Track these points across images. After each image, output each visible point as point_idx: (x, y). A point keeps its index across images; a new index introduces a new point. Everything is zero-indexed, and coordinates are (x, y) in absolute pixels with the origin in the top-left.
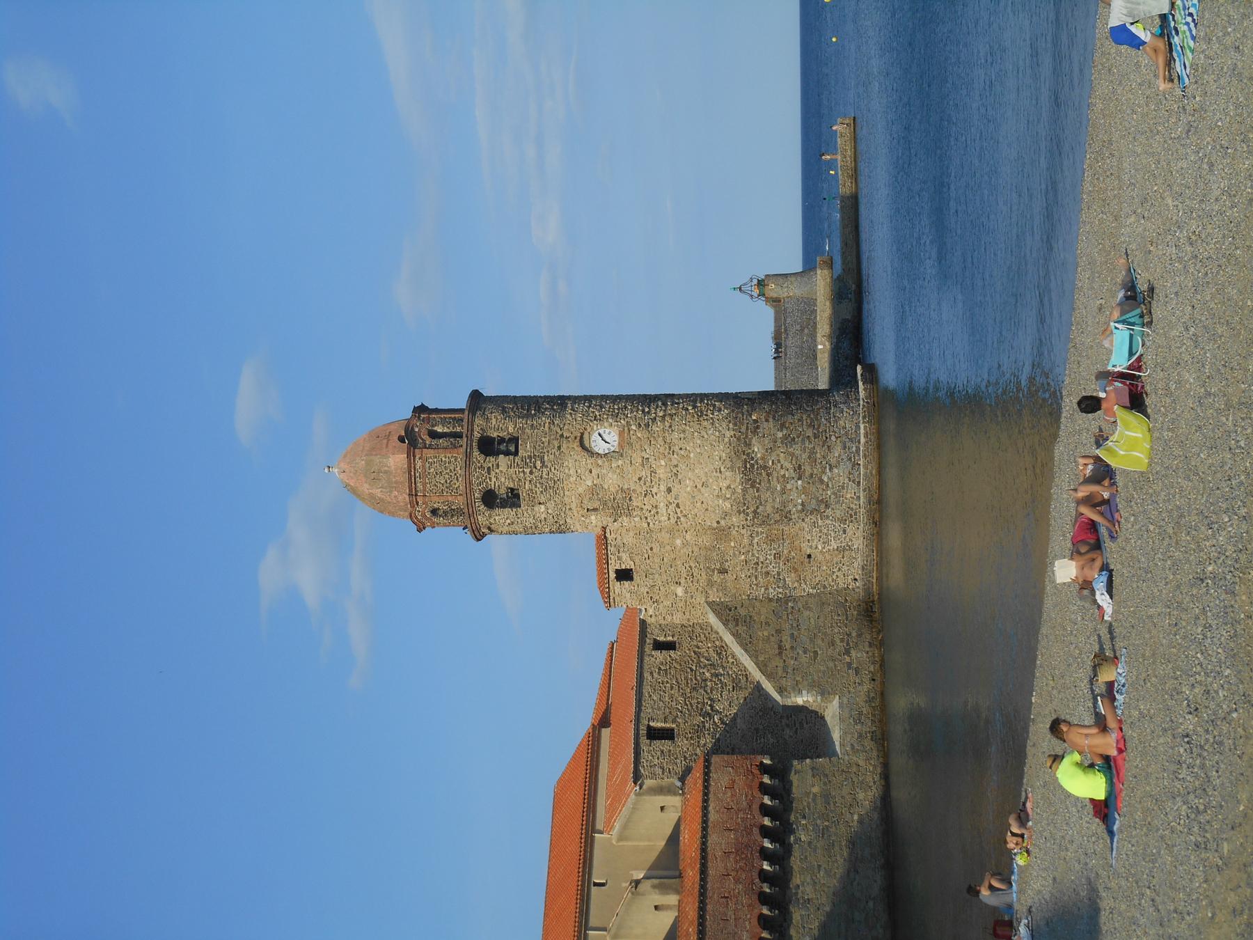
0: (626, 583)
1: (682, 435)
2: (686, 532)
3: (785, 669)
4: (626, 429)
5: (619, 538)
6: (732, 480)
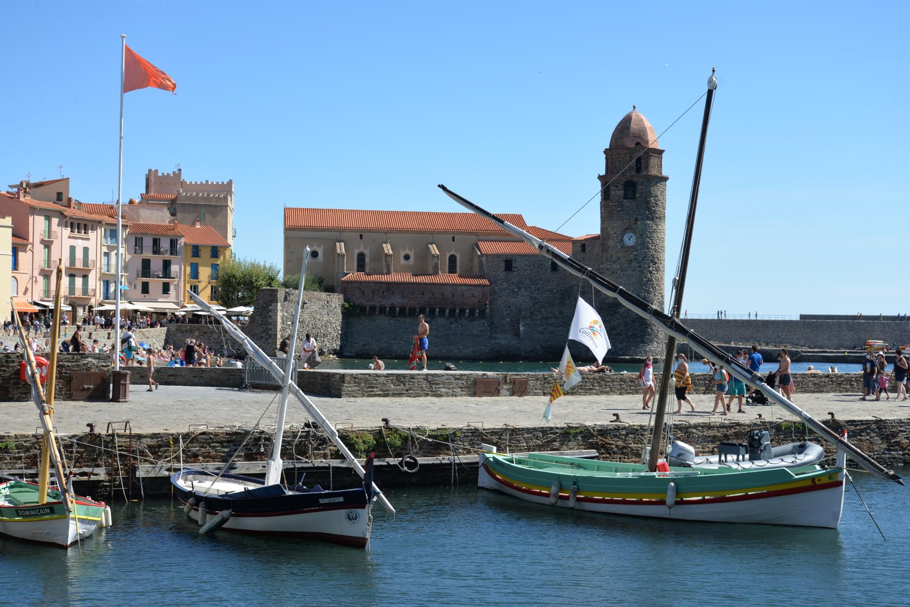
0: (580, 249)
3: (537, 320)
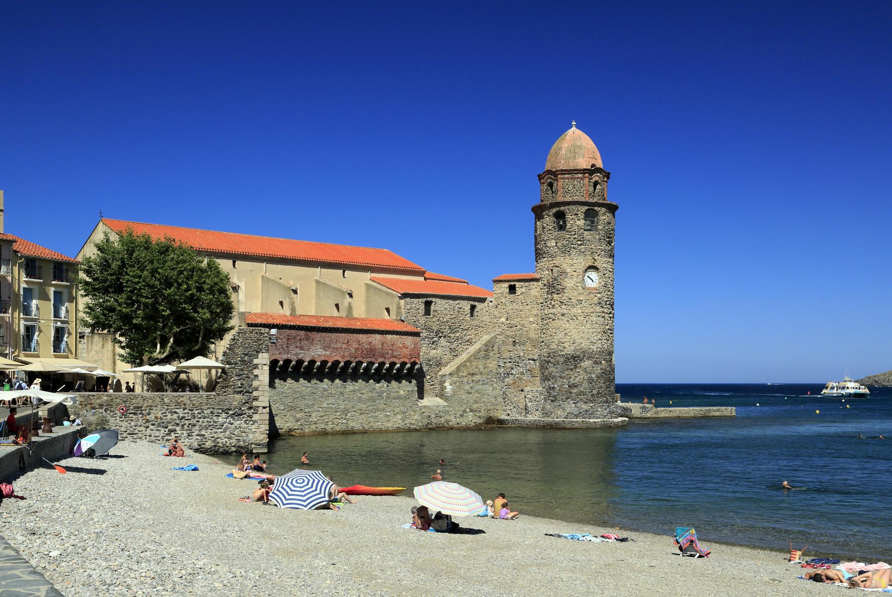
1: (594, 322)
2: (537, 324)
3: (463, 376)
4: (598, 291)
5: (534, 287)
6: (570, 350)
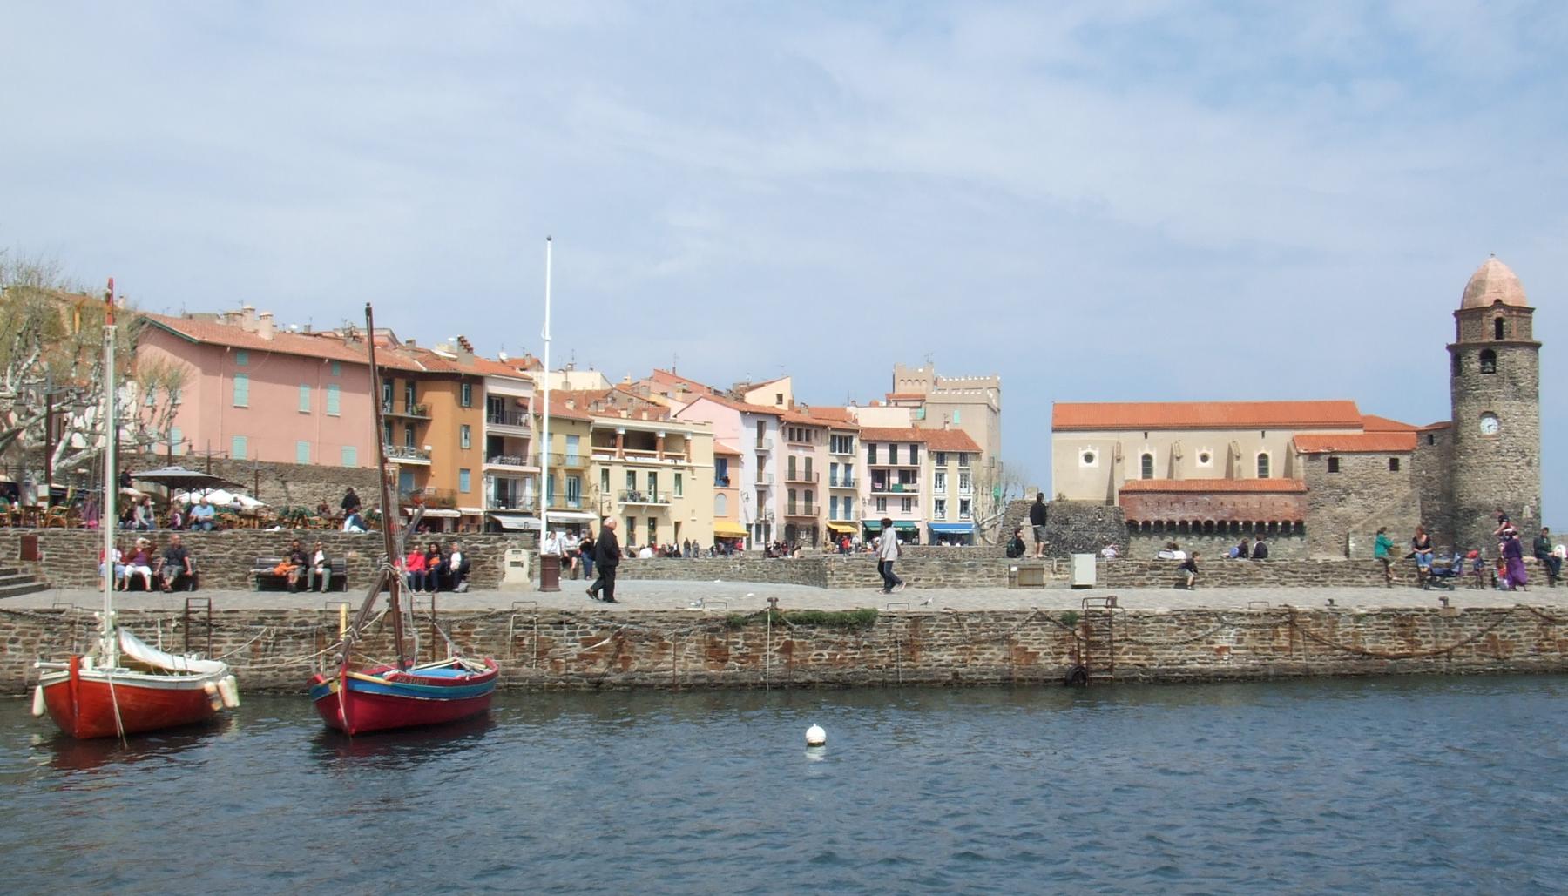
3: (1370, 534)
